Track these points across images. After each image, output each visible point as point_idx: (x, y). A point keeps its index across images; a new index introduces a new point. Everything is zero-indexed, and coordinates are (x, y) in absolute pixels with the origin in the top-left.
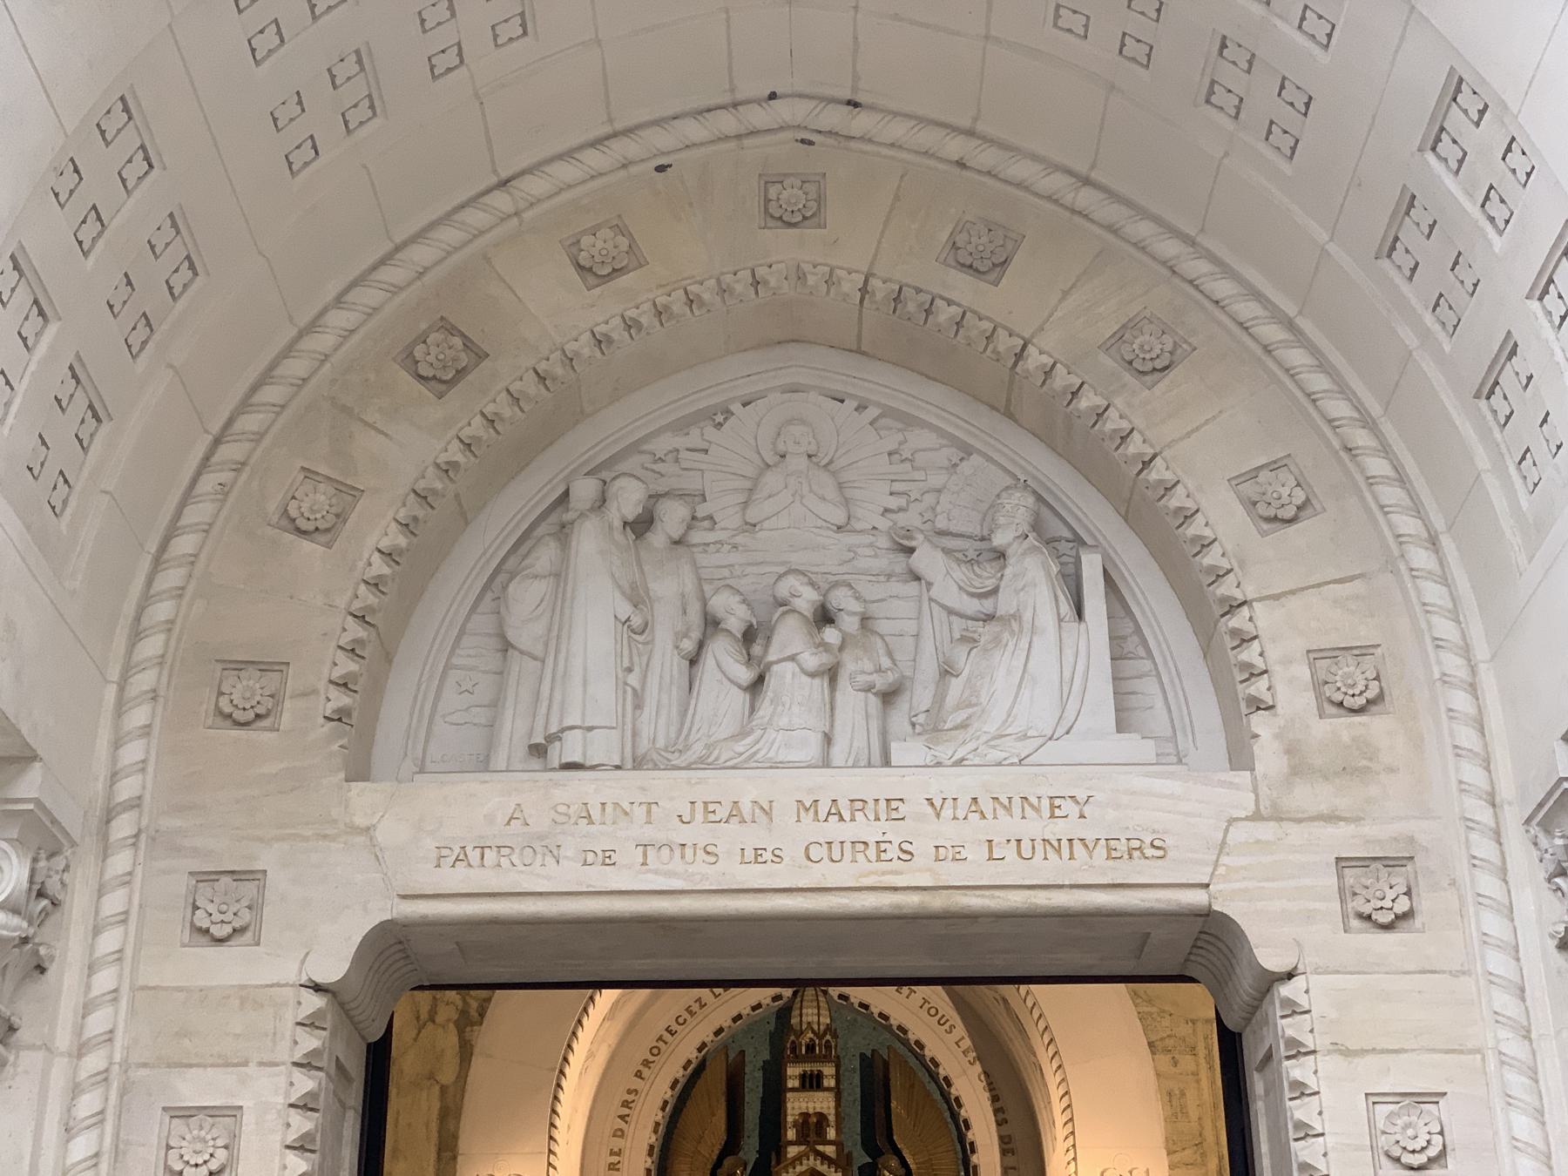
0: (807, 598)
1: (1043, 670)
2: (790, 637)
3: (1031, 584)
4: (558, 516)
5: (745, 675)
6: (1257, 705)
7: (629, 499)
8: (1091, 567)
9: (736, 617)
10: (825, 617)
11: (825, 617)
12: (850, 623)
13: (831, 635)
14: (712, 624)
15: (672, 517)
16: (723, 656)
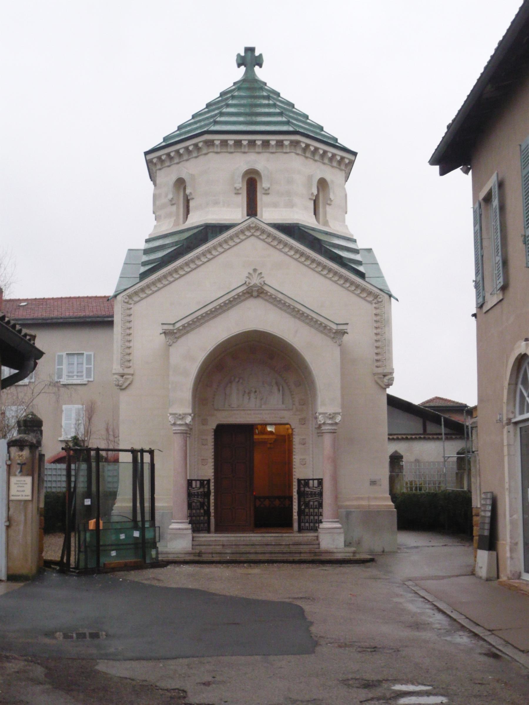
0: (254, 390)
1: (275, 400)
2: (252, 395)
3: (275, 389)
4: (231, 382)
5: (248, 398)
6: (294, 404)
7: (237, 380)
8: (281, 388)
9: (247, 391)
10: (256, 392)
11: (256, 392)
12: (258, 392)
13: (256, 394)
14: (245, 392)
15: (241, 381)
16: (246, 395)
